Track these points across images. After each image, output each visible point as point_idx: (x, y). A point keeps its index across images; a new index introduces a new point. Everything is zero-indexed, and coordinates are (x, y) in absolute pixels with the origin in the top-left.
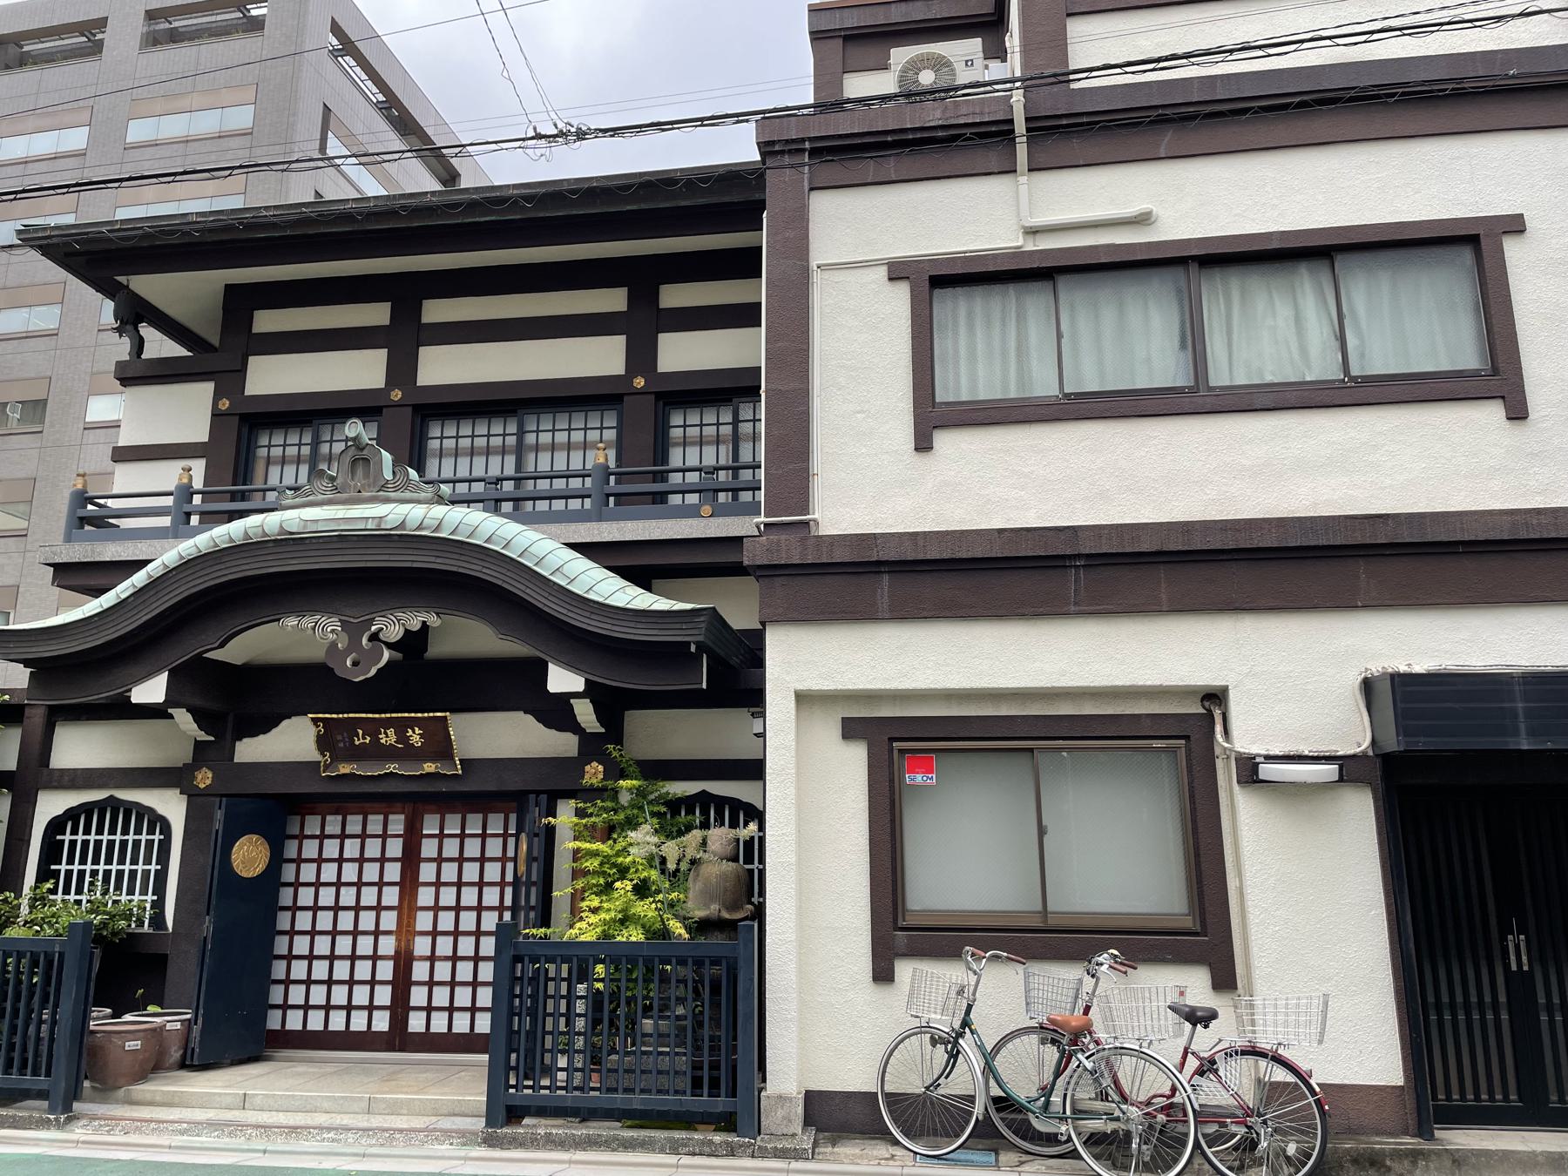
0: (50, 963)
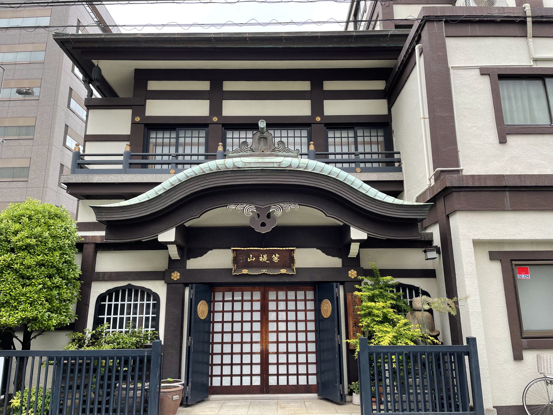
0: (141, 361)
